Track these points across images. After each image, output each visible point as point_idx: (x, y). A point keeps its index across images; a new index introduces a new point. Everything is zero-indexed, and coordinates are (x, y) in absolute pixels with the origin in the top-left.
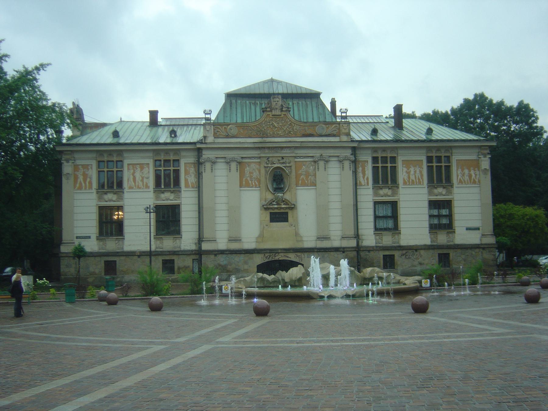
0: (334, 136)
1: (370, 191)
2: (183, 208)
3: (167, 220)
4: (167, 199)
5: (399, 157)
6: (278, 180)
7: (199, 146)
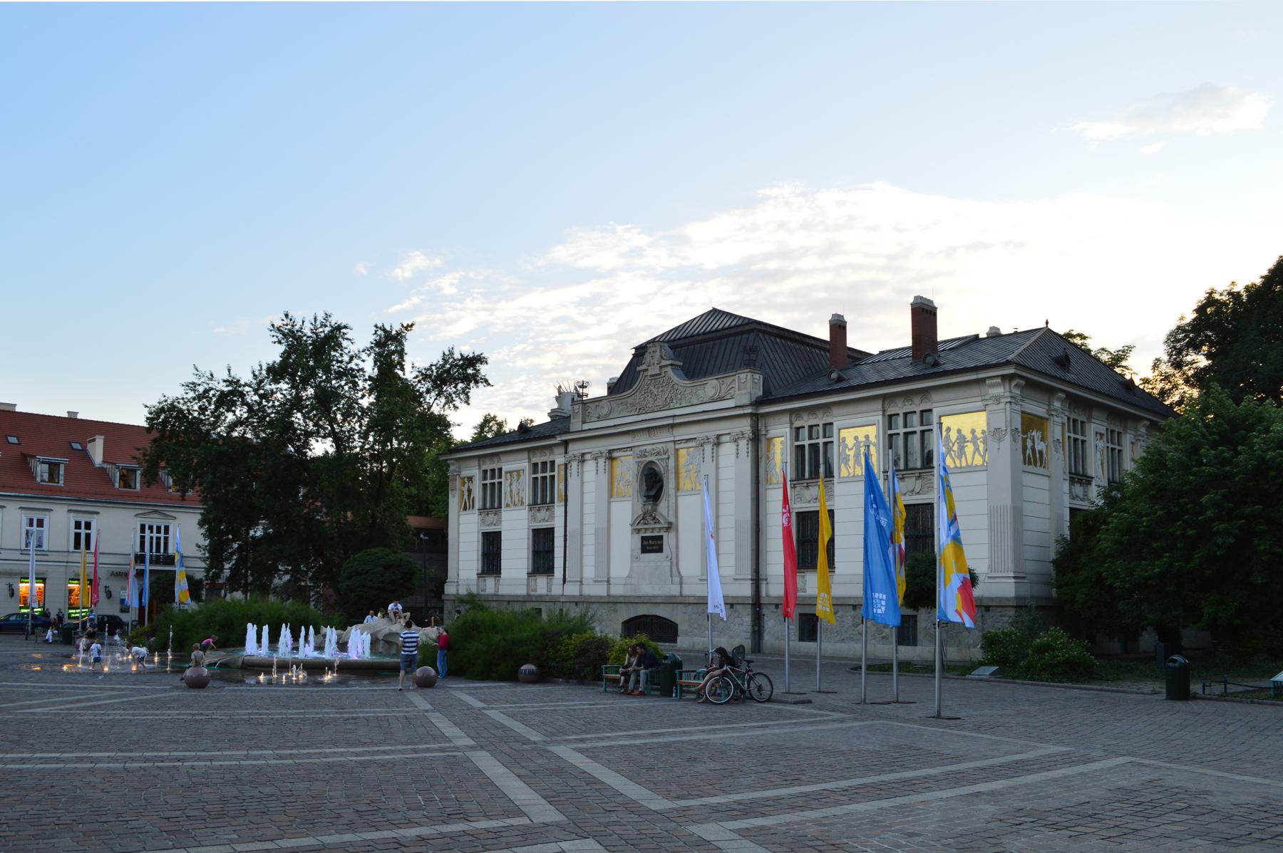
6: (653, 483)
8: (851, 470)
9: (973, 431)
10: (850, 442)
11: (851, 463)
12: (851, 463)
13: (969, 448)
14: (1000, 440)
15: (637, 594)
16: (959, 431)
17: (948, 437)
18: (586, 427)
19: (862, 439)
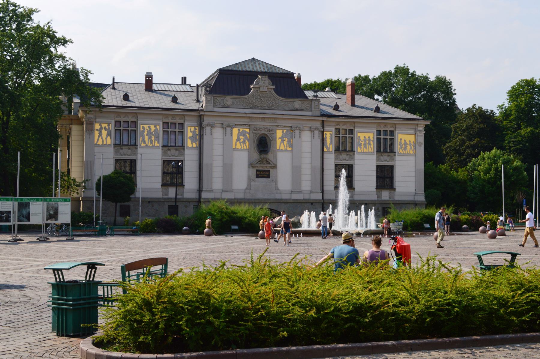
0: (307, 111)
1: (332, 156)
2: (186, 163)
3: (173, 173)
4: (173, 156)
5: (356, 130)
6: (263, 144)
7: (202, 113)
8: (362, 150)
9: (410, 141)
10: (362, 138)
11: (363, 147)
12: (363, 147)
13: (408, 147)
14: (420, 146)
15: (254, 198)
16: (405, 141)
17: (401, 142)
18: (216, 109)
19: (367, 138)
